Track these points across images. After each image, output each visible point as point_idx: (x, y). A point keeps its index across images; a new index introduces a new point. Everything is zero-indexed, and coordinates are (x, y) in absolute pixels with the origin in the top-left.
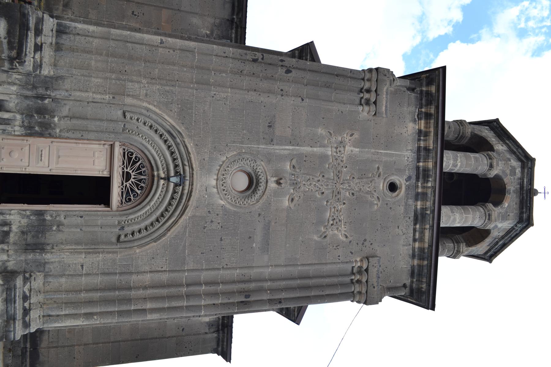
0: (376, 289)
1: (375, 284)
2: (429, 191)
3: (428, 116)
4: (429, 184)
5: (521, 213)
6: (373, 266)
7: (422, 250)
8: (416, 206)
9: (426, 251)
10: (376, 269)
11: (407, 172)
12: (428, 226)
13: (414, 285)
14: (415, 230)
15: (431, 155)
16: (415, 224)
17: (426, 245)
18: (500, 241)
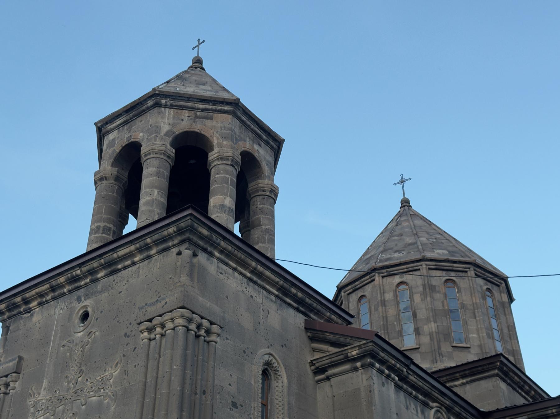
0: (167, 300)
1: (163, 302)
2: (85, 269)
3: (26, 302)
4: (78, 272)
5: (149, 109)
6: (145, 315)
7: (140, 250)
8: (103, 277)
9: (138, 245)
10: (149, 309)
11: (73, 305)
12: (115, 255)
13: (176, 242)
14: (125, 268)
15: (54, 283)
16: (119, 270)
17: (132, 248)
18: (198, 109)
